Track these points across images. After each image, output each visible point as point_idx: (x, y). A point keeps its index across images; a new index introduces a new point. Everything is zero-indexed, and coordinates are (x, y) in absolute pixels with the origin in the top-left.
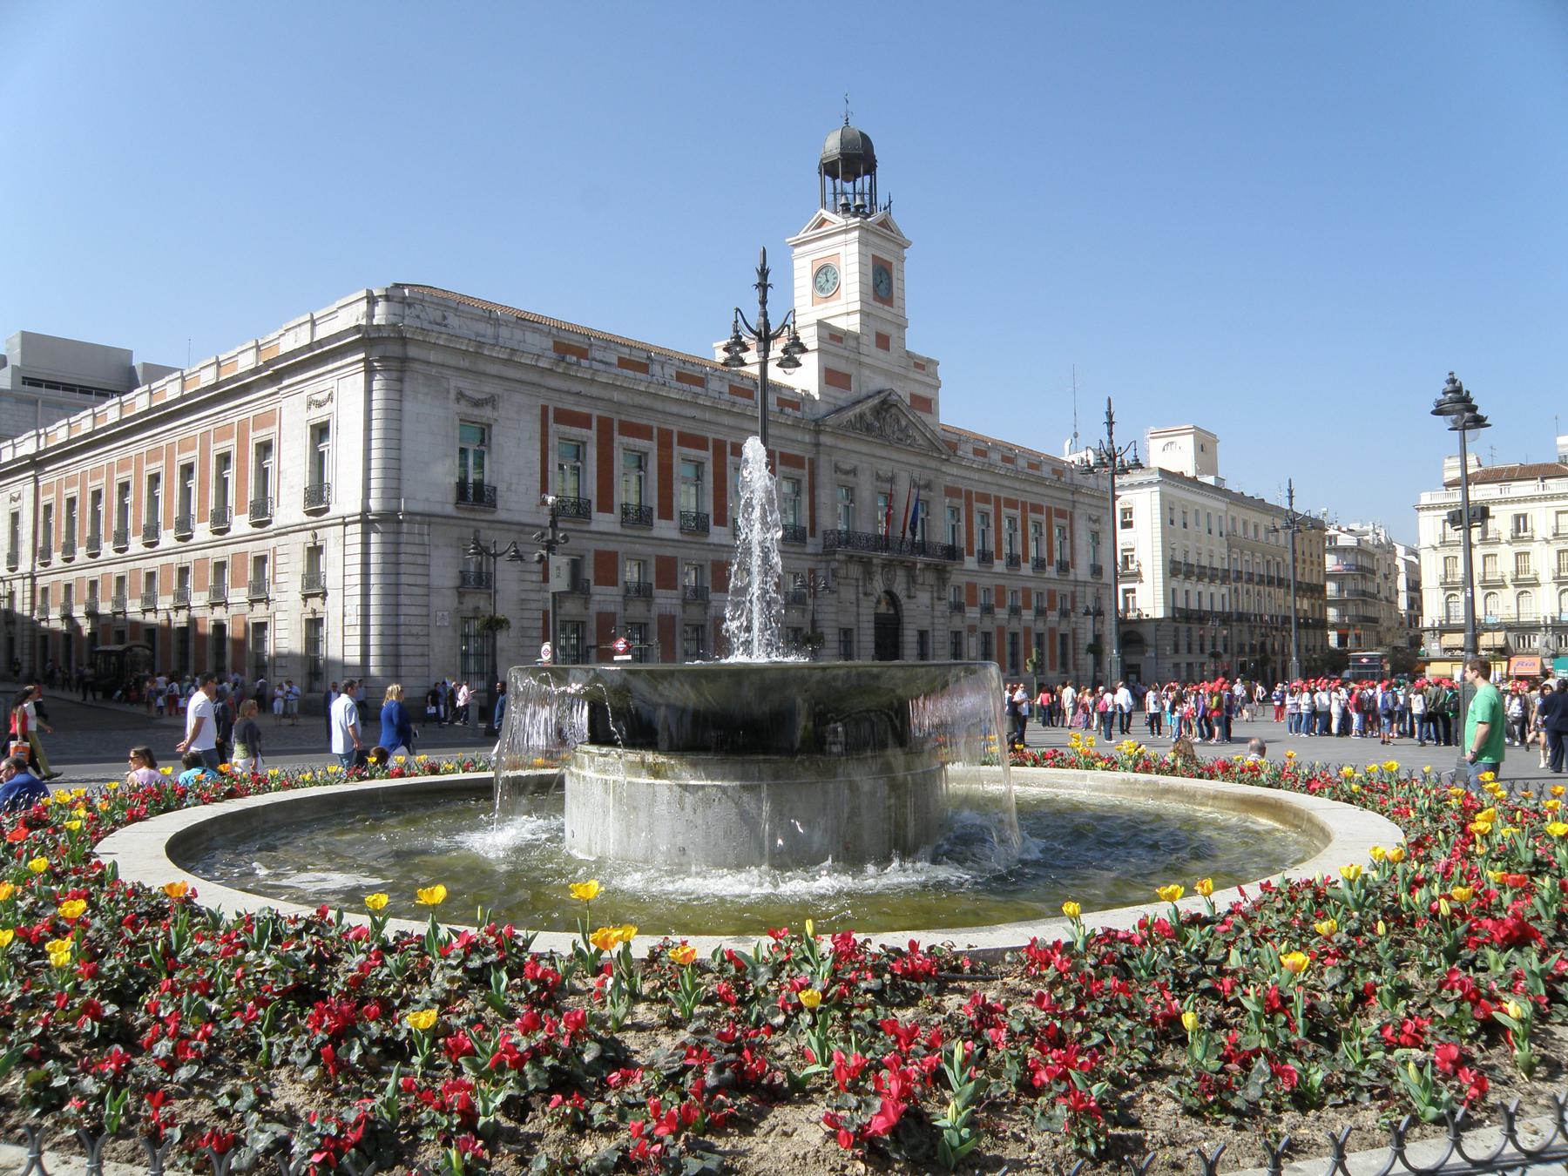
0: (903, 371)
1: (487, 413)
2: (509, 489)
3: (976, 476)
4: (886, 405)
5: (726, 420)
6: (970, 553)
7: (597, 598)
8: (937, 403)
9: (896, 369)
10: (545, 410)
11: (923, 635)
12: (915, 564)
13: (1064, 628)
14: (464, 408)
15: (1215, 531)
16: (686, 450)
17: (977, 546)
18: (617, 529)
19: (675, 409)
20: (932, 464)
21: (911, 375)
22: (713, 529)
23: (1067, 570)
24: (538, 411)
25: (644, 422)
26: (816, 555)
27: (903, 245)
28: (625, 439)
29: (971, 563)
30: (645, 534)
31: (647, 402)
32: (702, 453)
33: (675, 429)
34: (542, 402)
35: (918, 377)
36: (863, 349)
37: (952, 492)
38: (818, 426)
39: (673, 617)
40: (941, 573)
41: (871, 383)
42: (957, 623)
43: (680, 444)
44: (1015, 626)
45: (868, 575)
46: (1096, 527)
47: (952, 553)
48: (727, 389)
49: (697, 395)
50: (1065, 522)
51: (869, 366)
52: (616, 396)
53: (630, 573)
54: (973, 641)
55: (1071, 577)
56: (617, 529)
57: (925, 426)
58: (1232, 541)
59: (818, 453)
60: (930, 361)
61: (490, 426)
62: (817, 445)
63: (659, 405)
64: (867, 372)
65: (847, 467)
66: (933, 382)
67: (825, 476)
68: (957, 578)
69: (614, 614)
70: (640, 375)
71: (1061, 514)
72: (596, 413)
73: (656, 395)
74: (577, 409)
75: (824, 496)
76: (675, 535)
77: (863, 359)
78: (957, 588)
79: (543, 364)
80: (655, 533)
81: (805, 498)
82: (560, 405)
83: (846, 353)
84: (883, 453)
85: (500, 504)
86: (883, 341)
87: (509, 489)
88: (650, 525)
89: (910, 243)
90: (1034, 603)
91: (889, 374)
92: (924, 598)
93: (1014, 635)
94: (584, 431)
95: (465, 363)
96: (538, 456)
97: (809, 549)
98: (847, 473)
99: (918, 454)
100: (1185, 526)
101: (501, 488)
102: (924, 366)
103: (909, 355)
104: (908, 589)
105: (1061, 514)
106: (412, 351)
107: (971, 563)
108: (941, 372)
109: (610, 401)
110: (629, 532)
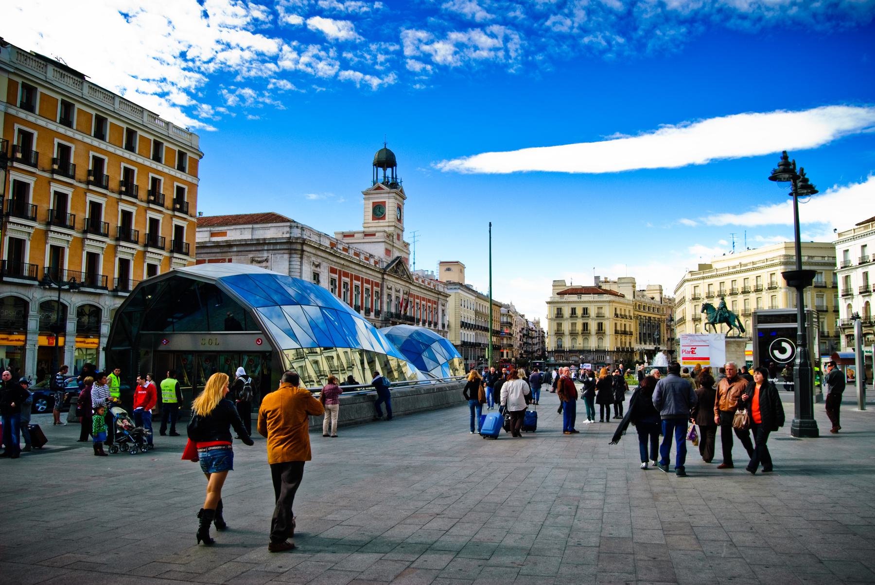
1: (318, 269)
14: (313, 268)
20: (408, 285)
38: (383, 272)
41: (396, 254)
58: (477, 313)
61: (318, 275)
62: (383, 278)
67: (385, 291)
71: (435, 303)
84: (397, 281)
95: (314, 251)
105: (435, 303)
106: (305, 248)
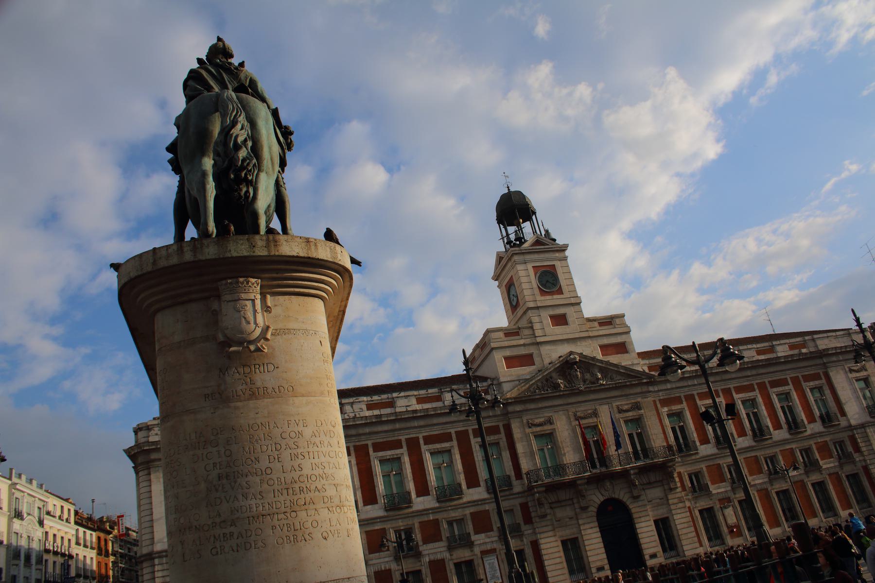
4: (567, 366)
9: (577, 336)
20: (638, 390)
26: (524, 492)
27: (563, 249)
39: (443, 561)
43: (375, 451)
45: (581, 495)
46: (863, 374)
62: (508, 413)
64: (545, 349)
65: (537, 421)
75: (520, 448)
76: (381, 513)
77: (539, 340)
83: (522, 342)
89: (566, 246)
98: (540, 425)
102: (608, 321)
103: (589, 320)
104: (631, 492)
108: (628, 320)
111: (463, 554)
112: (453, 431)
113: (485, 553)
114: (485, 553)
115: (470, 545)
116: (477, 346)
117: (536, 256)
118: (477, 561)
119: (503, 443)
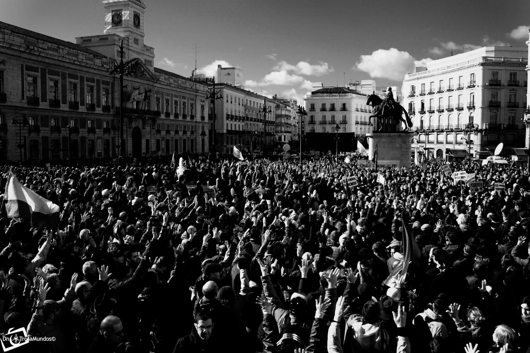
0: (142, 52)
2: (11, 94)
3: (165, 87)
5: (84, 69)
6: (163, 113)
7: (42, 132)
8: (153, 63)
10: (22, 65)
11: (148, 141)
12: (145, 117)
13: (192, 137)
15: (241, 104)
16: (71, 80)
17: (165, 111)
18: (48, 107)
19: (67, 65)
20: (151, 83)
21: (145, 53)
22: (80, 107)
23: (194, 118)
24: (20, 66)
25: (57, 70)
28: (50, 76)
29: (163, 116)
30: (57, 109)
31: (58, 63)
32: (77, 81)
33: (67, 72)
34: (21, 63)
35: (147, 54)
36: (130, 44)
37: (157, 93)
40: (154, 121)
42: (158, 137)
44: (177, 137)
46: (203, 104)
47: (158, 113)
48: (84, 58)
49: (75, 61)
50: (193, 102)
51: (131, 50)
52: (47, 61)
53: (53, 122)
54: (163, 142)
55: (195, 120)
56: (48, 107)
57: (149, 71)
58: (246, 107)
59: (114, 80)
60: (151, 48)
63: (62, 64)
64: (131, 52)
66: (152, 55)
68: (159, 122)
69: (48, 137)
70: (55, 53)
72: (40, 67)
73: (61, 61)
74: (33, 65)
76: (68, 109)
78: (159, 125)
79: (22, 49)
80: (61, 109)
81: (110, 96)
82: (28, 64)
85: (7, 99)
86: (136, 41)
87: (11, 94)
88: (59, 106)
90: (183, 129)
91: (138, 53)
92: (148, 128)
93: (176, 140)
94: (36, 73)
96: (20, 82)
97: (111, 113)
99: (147, 80)
100: (231, 102)
101: (8, 94)
102: (150, 49)
104: (143, 126)
107: (163, 116)
108: (155, 52)
109: (45, 63)
110: (52, 108)
111: (91, 136)
112: (96, 78)
113: (99, 138)
114: (99, 138)
115: (94, 133)
116: (98, 36)
117: (135, 6)
118: (95, 141)
119: (110, 91)
